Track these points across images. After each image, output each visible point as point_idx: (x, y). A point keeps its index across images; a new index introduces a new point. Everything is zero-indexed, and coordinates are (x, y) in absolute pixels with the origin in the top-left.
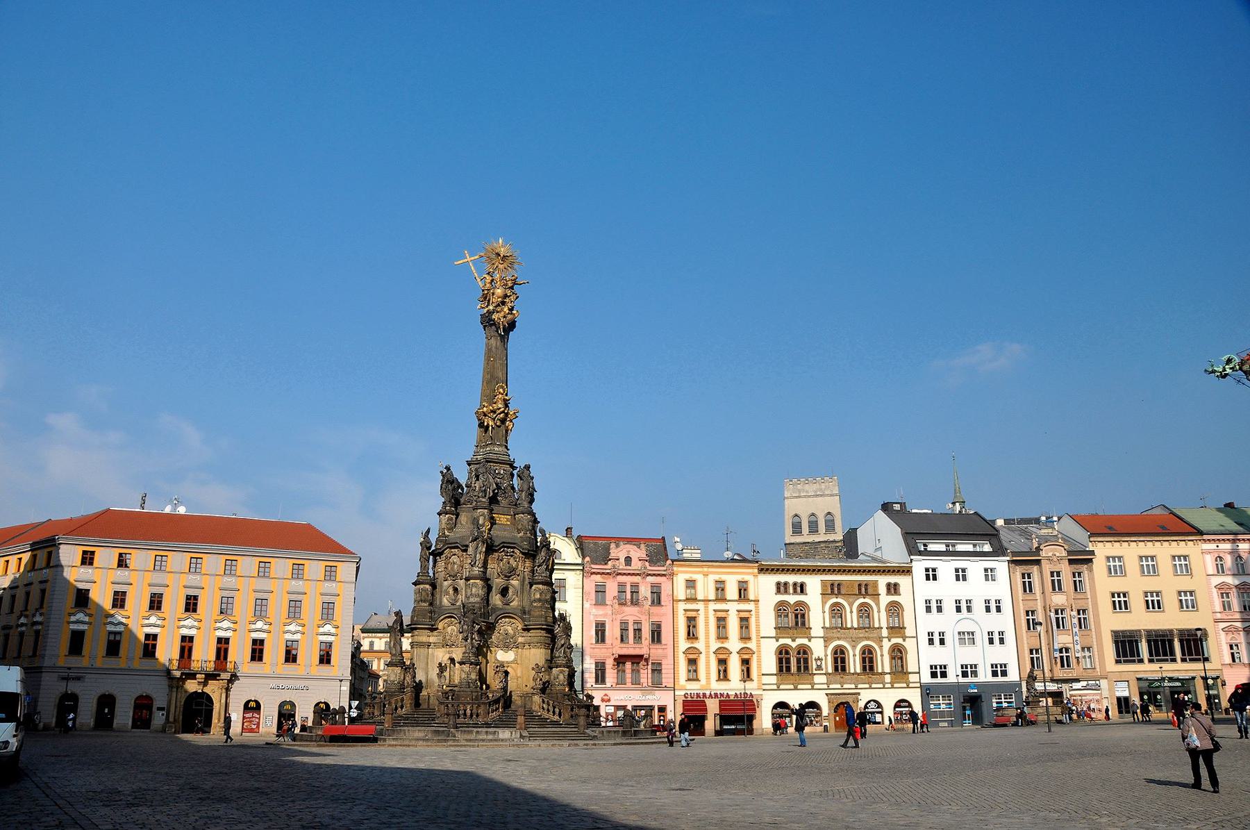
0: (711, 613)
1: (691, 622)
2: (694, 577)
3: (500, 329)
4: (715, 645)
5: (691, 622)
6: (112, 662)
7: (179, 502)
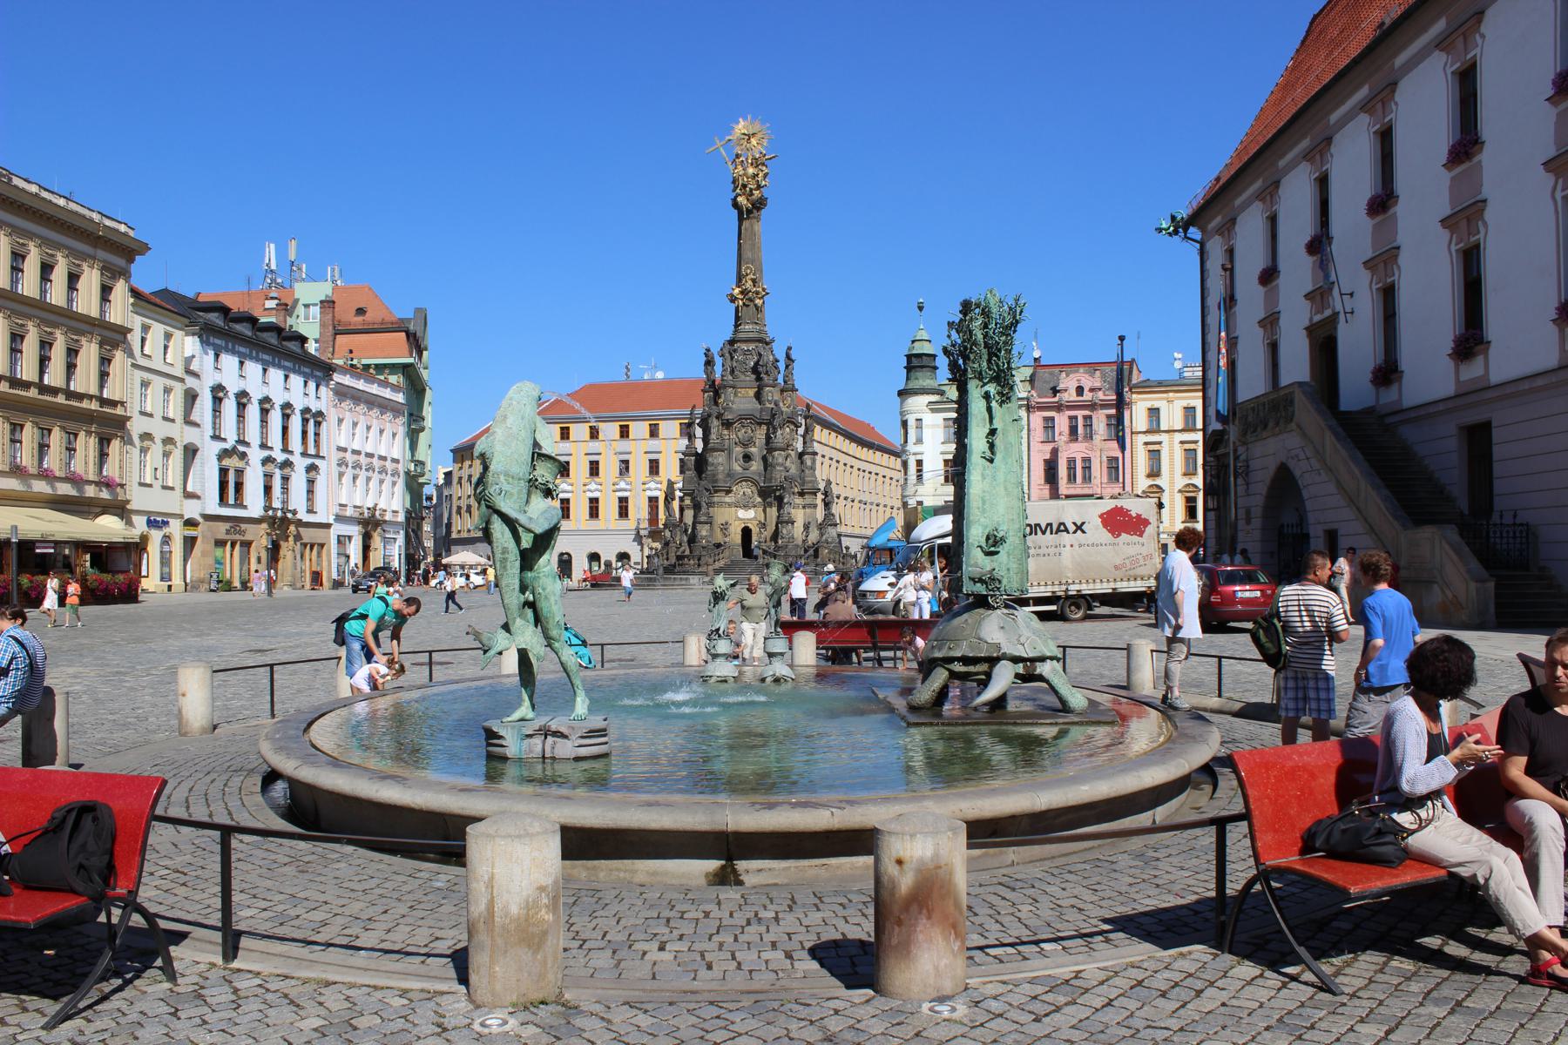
0: (1177, 447)
1: (1155, 456)
2: (1156, 404)
3: (749, 210)
4: (1181, 482)
5: (1155, 456)
6: (594, 524)
7: (656, 368)
